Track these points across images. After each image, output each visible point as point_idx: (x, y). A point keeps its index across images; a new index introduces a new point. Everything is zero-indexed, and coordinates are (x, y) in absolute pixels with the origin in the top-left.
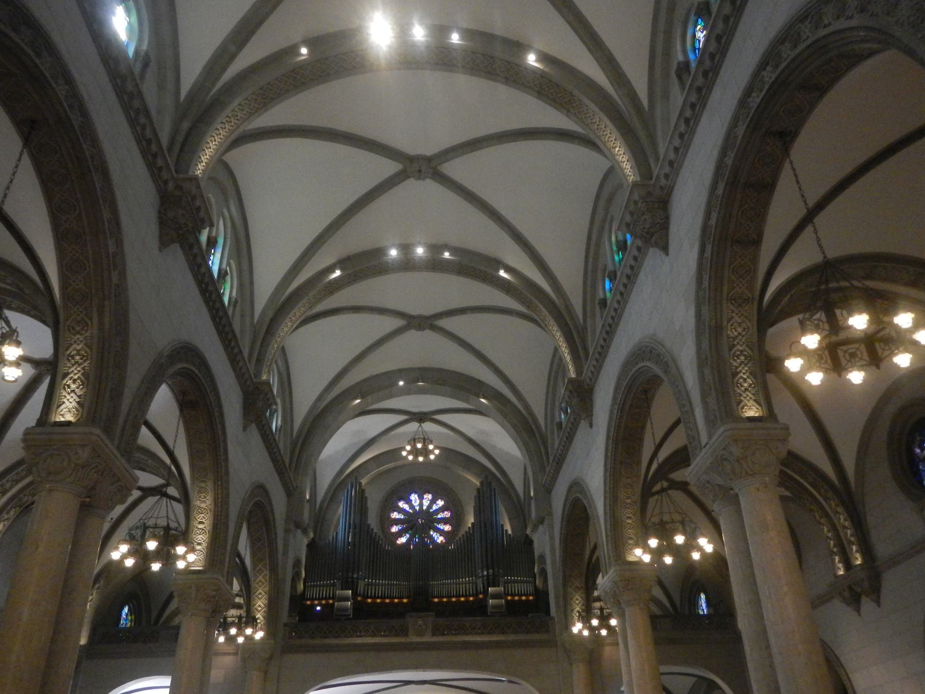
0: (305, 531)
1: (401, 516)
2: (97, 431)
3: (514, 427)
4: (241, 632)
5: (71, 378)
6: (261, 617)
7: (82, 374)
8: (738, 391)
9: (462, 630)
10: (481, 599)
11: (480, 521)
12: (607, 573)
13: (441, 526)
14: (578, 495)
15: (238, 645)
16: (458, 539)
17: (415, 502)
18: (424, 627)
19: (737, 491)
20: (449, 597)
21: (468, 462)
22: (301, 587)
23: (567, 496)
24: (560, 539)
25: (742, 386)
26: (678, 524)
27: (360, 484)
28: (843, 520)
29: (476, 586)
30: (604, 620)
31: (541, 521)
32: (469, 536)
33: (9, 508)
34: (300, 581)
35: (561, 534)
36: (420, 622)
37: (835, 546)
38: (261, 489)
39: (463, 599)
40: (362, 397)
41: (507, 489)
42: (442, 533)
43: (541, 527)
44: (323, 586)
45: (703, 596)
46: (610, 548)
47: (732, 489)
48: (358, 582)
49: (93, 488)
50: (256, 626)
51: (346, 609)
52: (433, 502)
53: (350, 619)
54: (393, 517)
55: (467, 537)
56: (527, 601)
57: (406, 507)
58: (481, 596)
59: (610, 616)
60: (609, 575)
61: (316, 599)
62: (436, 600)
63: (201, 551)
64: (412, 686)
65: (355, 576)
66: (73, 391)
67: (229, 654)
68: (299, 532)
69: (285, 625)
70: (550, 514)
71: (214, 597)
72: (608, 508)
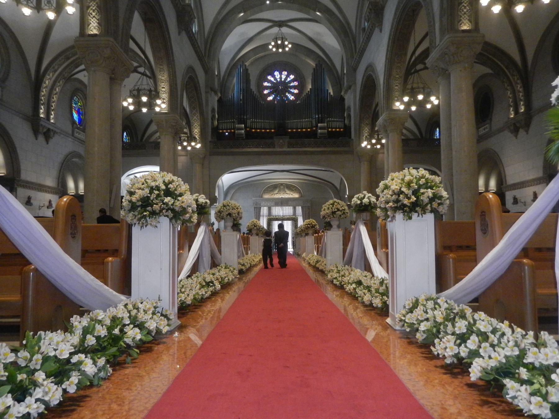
0: (216, 93)
1: (269, 85)
2: (112, 39)
3: (336, 30)
5: (91, 9)
7: (97, 7)
8: (460, 14)
10: (314, 130)
11: (315, 88)
13: (292, 91)
14: (371, 73)
17: (277, 75)
20: (297, 129)
21: (309, 52)
22: (216, 123)
23: (365, 71)
25: (463, 11)
26: (421, 89)
27: (245, 65)
28: (519, 87)
29: (312, 123)
30: (379, 141)
31: (349, 87)
32: (308, 96)
33: (59, 79)
34: (215, 120)
35: (360, 95)
36: (281, 141)
38: (191, 69)
39: (304, 130)
40: (245, 12)
41: (331, 68)
42: (293, 94)
43: (349, 90)
44: (228, 122)
46: (384, 102)
48: (247, 121)
49: (114, 70)
51: (242, 135)
52: (288, 76)
53: (244, 139)
54: (265, 85)
56: (340, 131)
57: (272, 79)
58: (314, 129)
59: (382, 138)
62: (290, 130)
64: (278, 173)
66: (94, 17)
67: (183, 156)
69: (210, 142)
70: (355, 83)
71: (175, 126)
72: (385, 81)
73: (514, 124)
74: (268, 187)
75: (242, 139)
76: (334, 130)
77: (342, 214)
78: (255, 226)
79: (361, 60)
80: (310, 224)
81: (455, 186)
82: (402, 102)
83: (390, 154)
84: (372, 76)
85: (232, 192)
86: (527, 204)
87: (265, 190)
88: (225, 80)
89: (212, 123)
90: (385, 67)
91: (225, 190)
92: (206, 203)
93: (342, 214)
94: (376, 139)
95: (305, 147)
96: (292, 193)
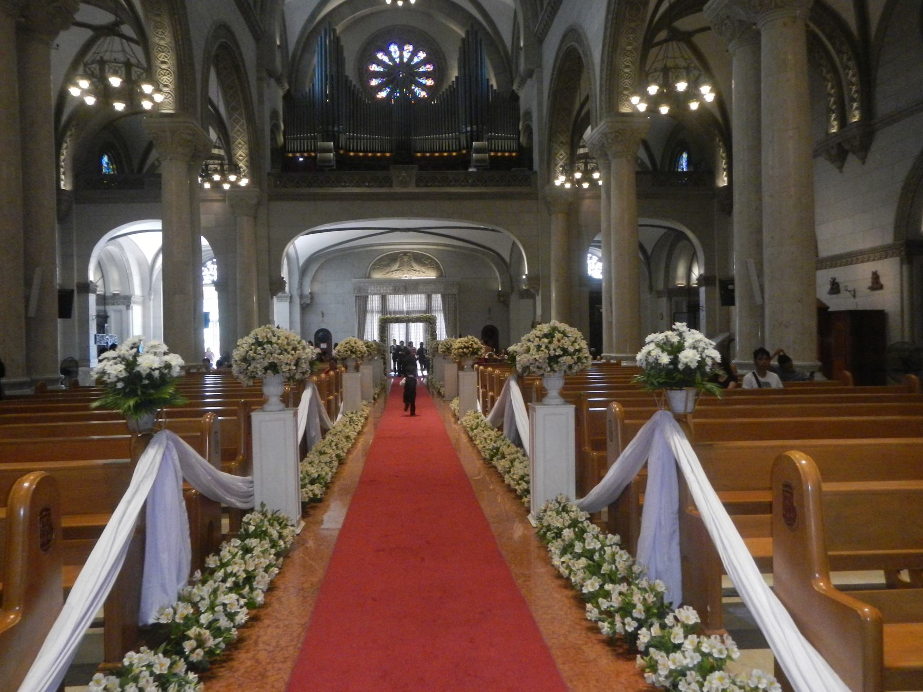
0: (279, 81)
1: (379, 69)
4: (225, 180)
6: (244, 166)
9: (446, 182)
10: (464, 155)
11: (465, 76)
12: (597, 126)
13: (424, 81)
14: (573, 43)
15: (225, 191)
16: (441, 93)
17: (395, 52)
18: (408, 179)
19: (759, 26)
20: (432, 151)
22: (281, 139)
23: (562, 42)
24: (549, 93)
27: (334, 31)
28: (851, 75)
30: (587, 176)
31: (530, 74)
32: (453, 91)
34: (279, 134)
35: (550, 89)
36: (404, 174)
37: (835, 103)
38: (223, 29)
39: (445, 154)
41: (495, 40)
42: (424, 87)
43: (529, 81)
45: (685, 156)
46: (603, 98)
47: (755, 24)
48: (339, 137)
50: (240, 173)
51: (330, 161)
52: (414, 54)
53: (333, 170)
55: (451, 93)
56: (510, 157)
57: (386, 59)
58: (464, 152)
59: (593, 170)
60: (599, 127)
61: (297, 152)
62: (419, 155)
63: (169, 93)
64: (398, 233)
65: (336, 129)
68: (272, 81)
69: (269, 174)
70: (540, 66)
73: (839, 144)
74: (382, 258)
75: (329, 170)
76: (499, 154)
77: (576, 363)
78: (352, 352)
79: (552, 21)
80: (467, 348)
81: (767, 270)
82: (645, 97)
83: (613, 200)
84: (575, 50)
85: (314, 268)
86: (857, 293)
87: (373, 265)
88: (298, 58)
89: (274, 139)
90: (606, 29)
91: (300, 265)
92: (168, 366)
93: (576, 363)
94: (581, 172)
95: (449, 185)
96: (424, 270)
